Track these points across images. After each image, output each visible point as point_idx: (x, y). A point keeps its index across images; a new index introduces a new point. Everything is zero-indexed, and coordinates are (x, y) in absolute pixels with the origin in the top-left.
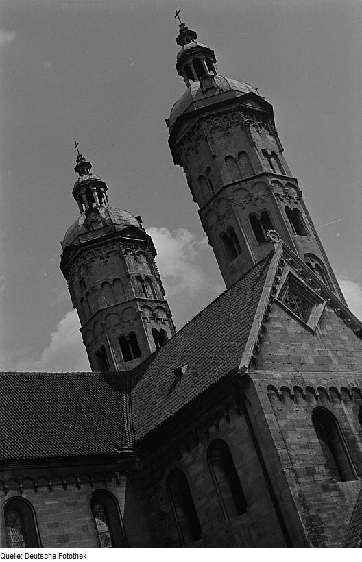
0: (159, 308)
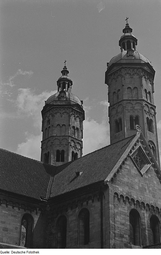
0: (78, 143)
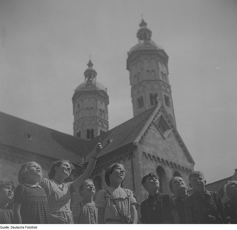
0: (105, 123)
